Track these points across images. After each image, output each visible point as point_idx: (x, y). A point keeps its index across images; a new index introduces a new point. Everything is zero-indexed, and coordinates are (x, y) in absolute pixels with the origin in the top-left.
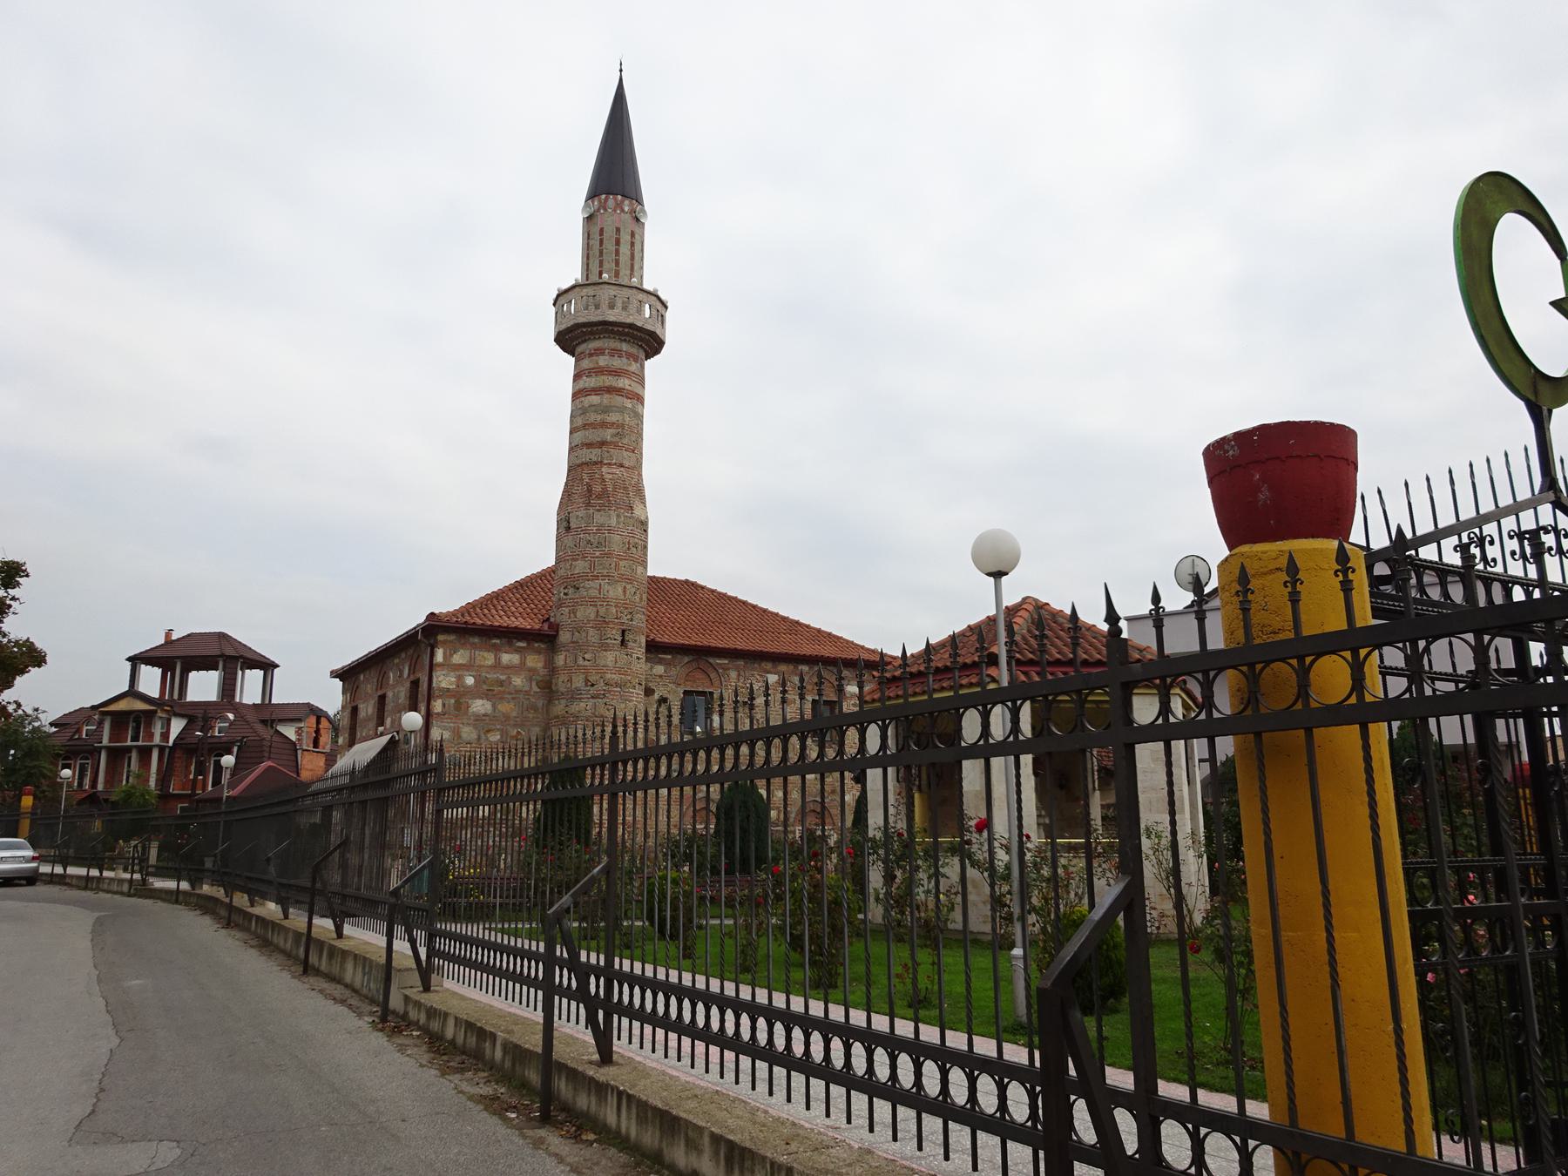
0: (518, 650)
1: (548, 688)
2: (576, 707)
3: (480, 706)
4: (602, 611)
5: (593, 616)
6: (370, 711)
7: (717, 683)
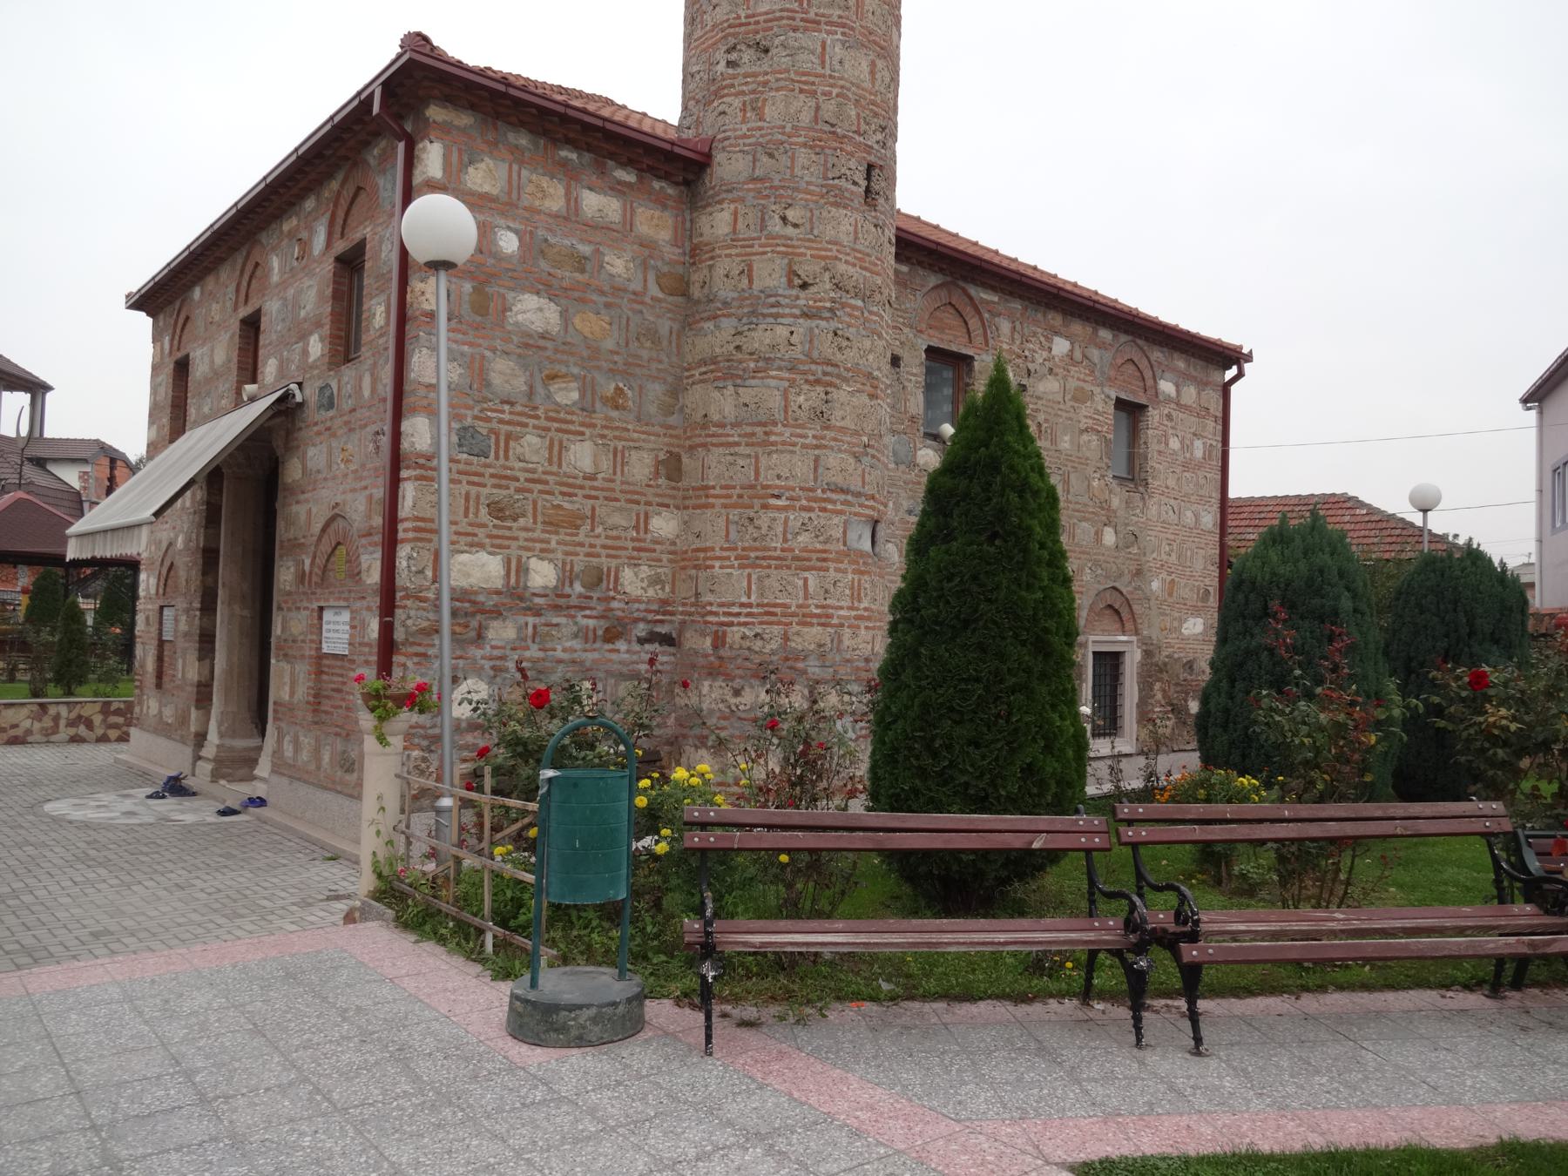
0: (618, 189)
1: (685, 293)
2: (760, 339)
3: (533, 311)
4: (829, 110)
5: (806, 118)
6: (220, 356)
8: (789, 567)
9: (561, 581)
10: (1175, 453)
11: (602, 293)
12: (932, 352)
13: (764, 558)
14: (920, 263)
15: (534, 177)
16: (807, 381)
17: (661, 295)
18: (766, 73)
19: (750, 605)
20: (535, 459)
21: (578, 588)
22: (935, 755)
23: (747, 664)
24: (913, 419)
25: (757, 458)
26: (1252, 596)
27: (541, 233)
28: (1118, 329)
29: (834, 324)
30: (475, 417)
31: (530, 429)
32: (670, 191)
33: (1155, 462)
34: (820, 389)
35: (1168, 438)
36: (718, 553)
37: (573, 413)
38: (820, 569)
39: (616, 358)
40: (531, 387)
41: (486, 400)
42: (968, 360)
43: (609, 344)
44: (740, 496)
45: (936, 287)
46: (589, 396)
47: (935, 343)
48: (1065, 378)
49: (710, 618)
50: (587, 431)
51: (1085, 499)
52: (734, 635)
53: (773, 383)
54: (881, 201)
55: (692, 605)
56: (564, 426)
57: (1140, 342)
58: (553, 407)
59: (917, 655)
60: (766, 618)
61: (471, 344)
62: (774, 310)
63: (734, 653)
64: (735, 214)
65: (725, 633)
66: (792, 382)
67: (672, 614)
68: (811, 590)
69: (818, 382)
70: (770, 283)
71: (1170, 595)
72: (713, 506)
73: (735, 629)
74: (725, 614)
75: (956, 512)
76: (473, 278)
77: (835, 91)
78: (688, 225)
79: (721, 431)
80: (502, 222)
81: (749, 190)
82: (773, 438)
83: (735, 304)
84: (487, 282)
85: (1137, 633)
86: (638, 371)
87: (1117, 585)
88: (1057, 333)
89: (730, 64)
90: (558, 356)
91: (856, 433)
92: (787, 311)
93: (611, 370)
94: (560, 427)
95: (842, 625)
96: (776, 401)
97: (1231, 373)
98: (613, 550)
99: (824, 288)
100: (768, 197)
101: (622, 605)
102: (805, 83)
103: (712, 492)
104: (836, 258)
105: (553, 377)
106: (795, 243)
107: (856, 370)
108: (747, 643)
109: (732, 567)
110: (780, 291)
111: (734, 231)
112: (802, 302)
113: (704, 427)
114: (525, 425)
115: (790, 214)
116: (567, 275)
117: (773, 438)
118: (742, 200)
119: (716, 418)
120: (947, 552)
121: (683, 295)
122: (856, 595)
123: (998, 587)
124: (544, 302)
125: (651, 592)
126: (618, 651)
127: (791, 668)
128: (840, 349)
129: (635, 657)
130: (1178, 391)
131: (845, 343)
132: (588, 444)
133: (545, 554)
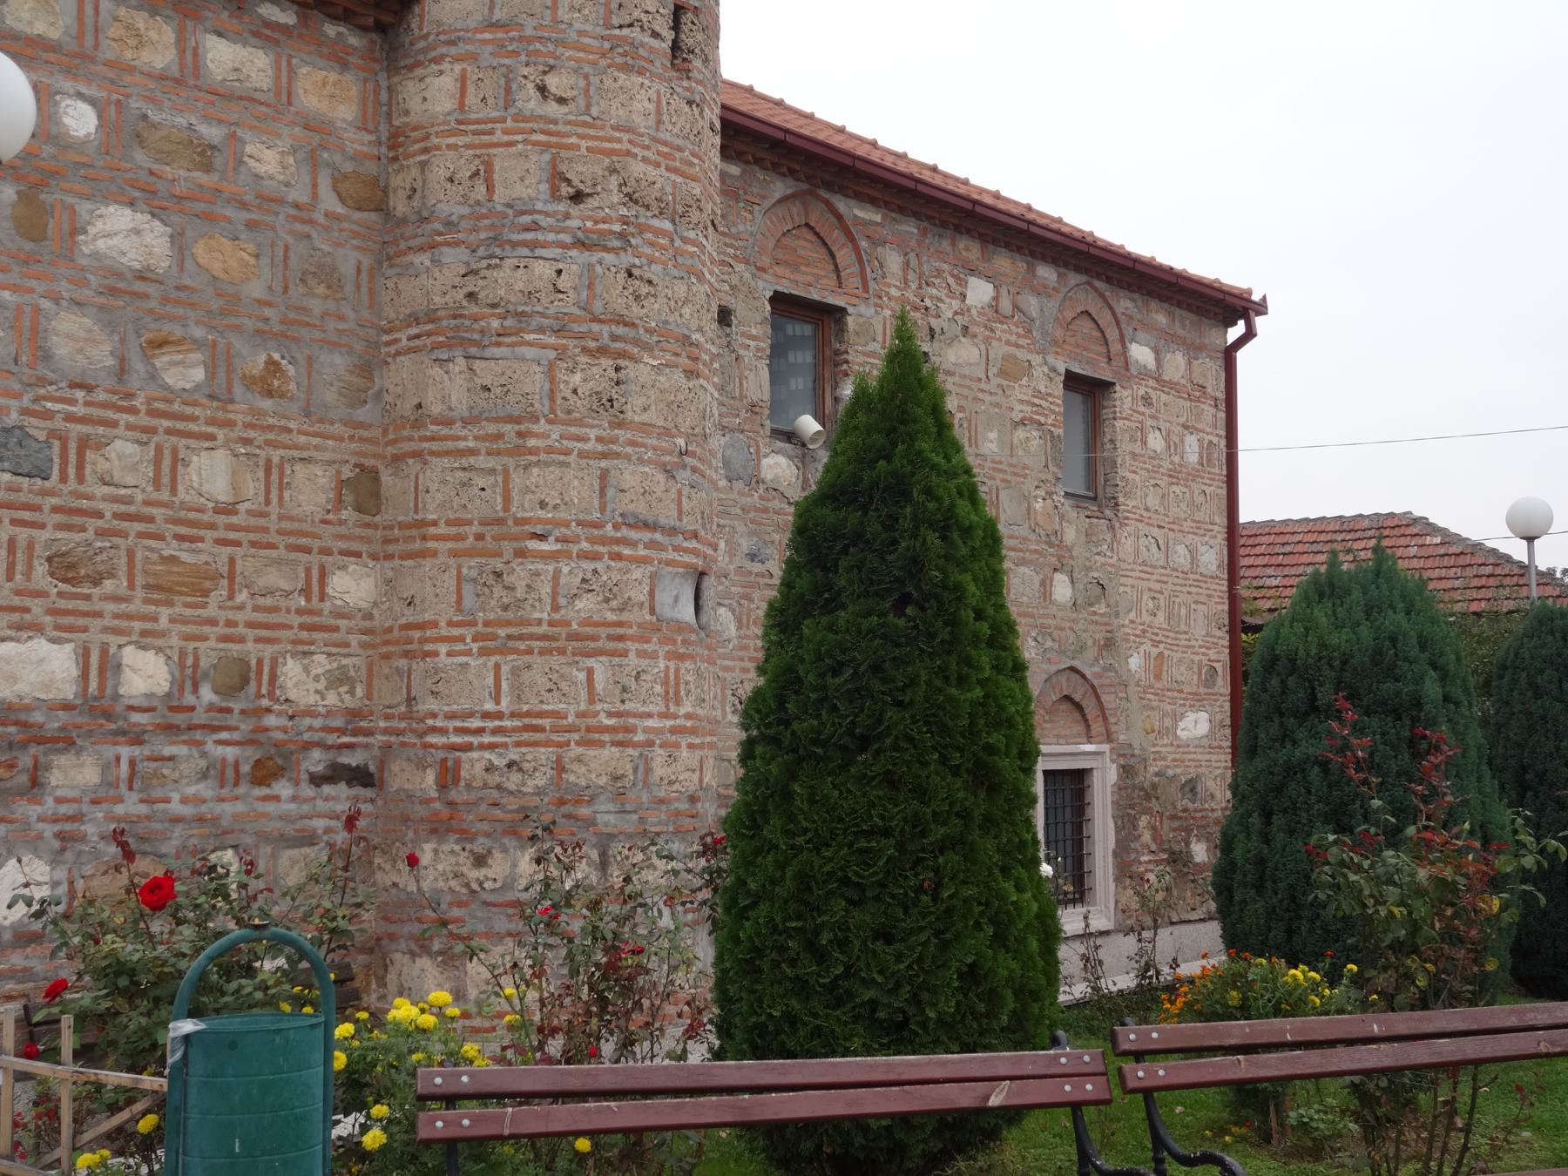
0: (267, 35)
2: (507, 281)
3: (121, 234)
7: (853, 282)
8: (562, 652)
9: (178, 685)
10: (1155, 456)
11: (243, 205)
12: (781, 302)
13: (521, 638)
14: (758, 161)
15: (122, 12)
16: (585, 350)
17: (340, 209)
19: (499, 715)
20: (130, 480)
21: (207, 695)
22: (821, 957)
23: (497, 812)
24: (753, 408)
25: (506, 472)
26: (1292, 682)
27: (135, 104)
28: (1066, 265)
29: (627, 259)
30: (25, 412)
31: (120, 431)
32: (354, 40)
33: (1129, 473)
34: (607, 362)
35: (1147, 433)
36: (444, 632)
37: (195, 404)
38: (613, 653)
39: (267, 312)
40: (122, 360)
41: (43, 381)
42: (835, 315)
43: (256, 289)
44: (480, 537)
45: (780, 201)
46: (222, 375)
47: (786, 288)
48: (987, 341)
49: (432, 739)
50: (221, 434)
51: (1024, 531)
52: (474, 765)
53: (530, 352)
54: (697, 63)
55: (402, 717)
56: (180, 425)
57: (1097, 284)
58: (161, 393)
59: (788, 795)
60: (526, 736)
61: (15, 289)
62: (529, 236)
63: (474, 796)
64: (463, 79)
65: (458, 763)
66: (562, 353)
67: (368, 733)
68: (599, 687)
69: (603, 351)
70: (520, 191)
71: (1158, 677)
72: (434, 554)
73: (475, 755)
74: (458, 731)
75: (843, 563)
76: (18, 178)
78: (384, 96)
79: (445, 431)
80: (68, 85)
81: (485, 42)
82: (532, 442)
83: (464, 224)
84: (42, 184)
85: (1109, 738)
86: (305, 333)
87: (1077, 664)
88: (973, 272)
90: (169, 308)
91: (666, 432)
92: (551, 237)
93: (259, 332)
94: (173, 427)
95: (651, 744)
96: (535, 383)
97: (1236, 331)
98: (266, 630)
99: (610, 198)
100: (515, 53)
101: (283, 721)
103: (432, 530)
104: (628, 153)
105: (160, 344)
106: (561, 128)
107: (663, 331)
108: (495, 779)
109: (468, 653)
110: (539, 206)
111: (462, 105)
112: (574, 223)
113: (417, 424)
114: (114, 424)
115: (553, 82)
116: (182, 175)
117: (532, 442)
118: (473, 58)
119: (436, 409)
120: (830, 628)
121: (378, 210)
122: (673, 694)
123: (913, 682)
124: (142, 218)
125: (332, 699)
126: (277, 798)
127: (569, 816)
128: (637, 298)
129: (306, 808)
130: (1158, 360)
131: (645, 289)
132: (221, 454)
133: (148, 639)
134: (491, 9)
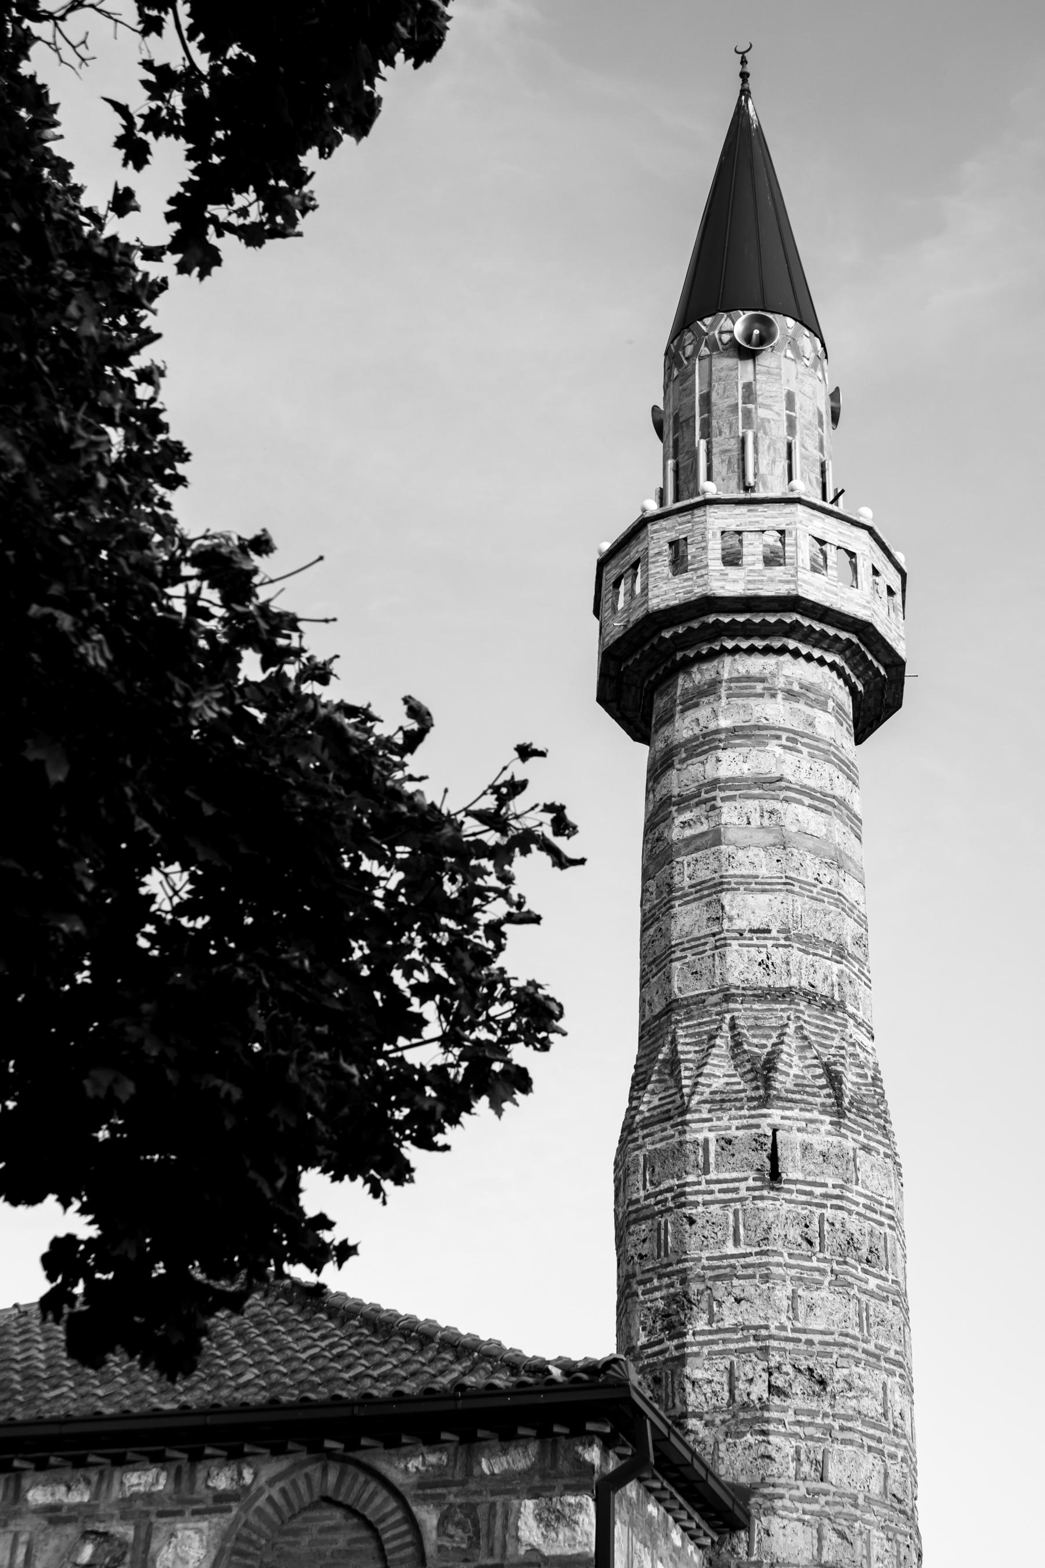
5: (876, 1487)
18: (825, 1415)
77: (900, 1453)
89: (772, 1389)
102: (872, 1437)
134: (820, 1549)
